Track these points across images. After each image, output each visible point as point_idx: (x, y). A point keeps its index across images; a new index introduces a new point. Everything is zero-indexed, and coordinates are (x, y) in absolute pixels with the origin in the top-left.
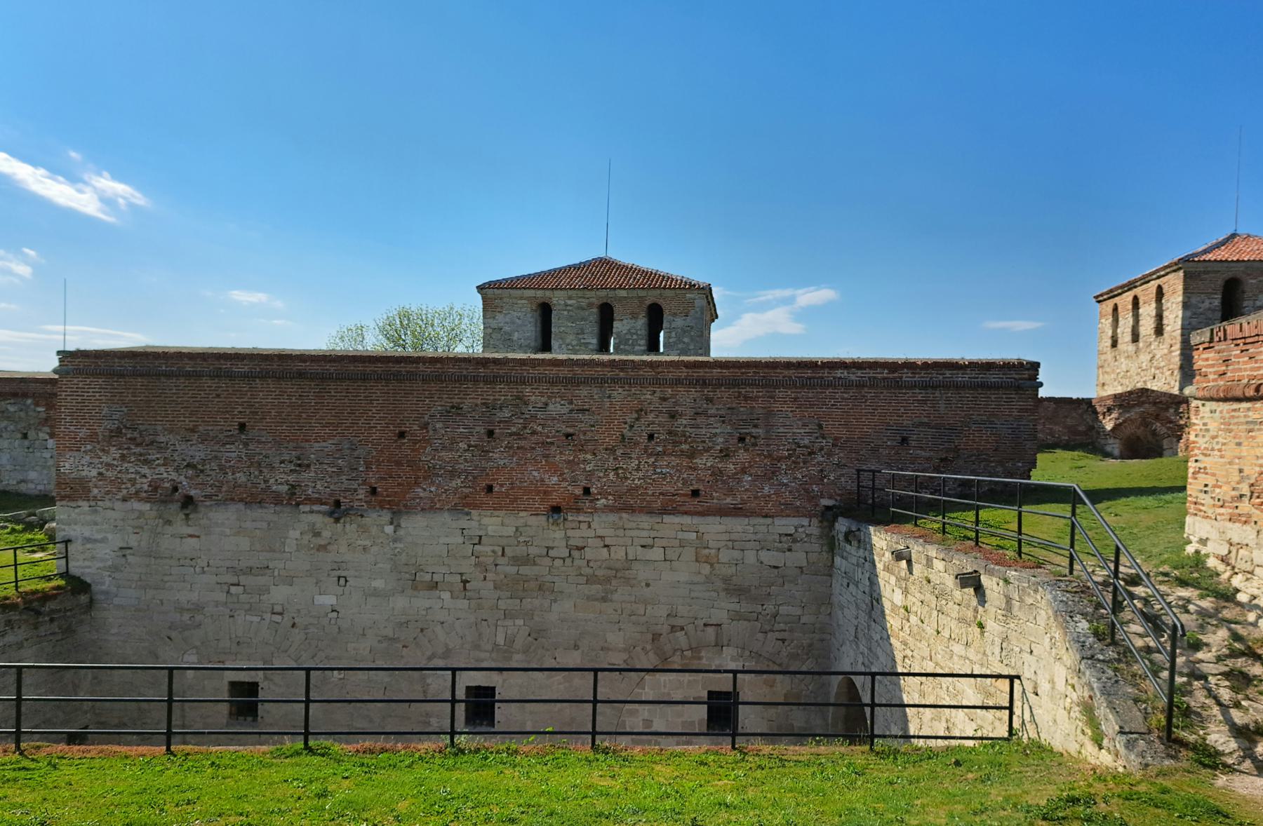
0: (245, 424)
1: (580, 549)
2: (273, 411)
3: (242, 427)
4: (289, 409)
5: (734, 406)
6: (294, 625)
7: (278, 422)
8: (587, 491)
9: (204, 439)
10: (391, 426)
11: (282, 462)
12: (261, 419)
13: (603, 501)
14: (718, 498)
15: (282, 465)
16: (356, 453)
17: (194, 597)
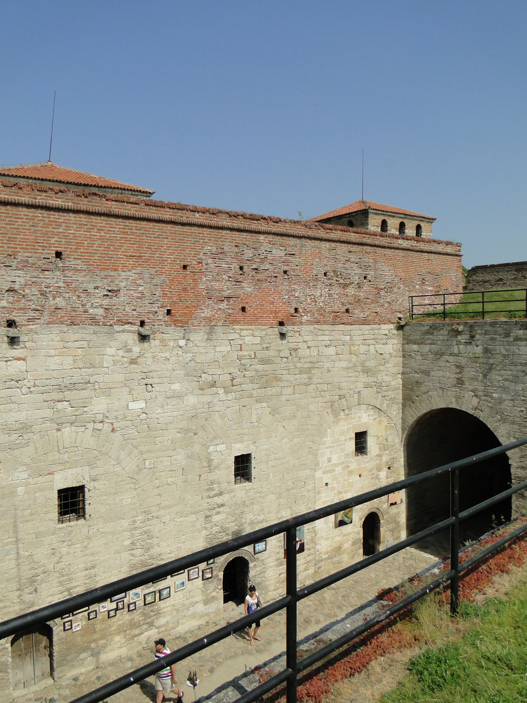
0: (61, 253)
1: (295, 350)
2: (86, 242)
3: (58, 255)
4: (99, 242)
5: (361, 257)
6: (113, 430)
7: (90, 253)
8: (296, 310)
9: (25, 265)
10: (178, 260)
11: (96, 288)
12: (76, 249)
13: (305, 317)
14: (358, 313)
15: (97, 291)
16: (154, 281)
17: (22, 416)
